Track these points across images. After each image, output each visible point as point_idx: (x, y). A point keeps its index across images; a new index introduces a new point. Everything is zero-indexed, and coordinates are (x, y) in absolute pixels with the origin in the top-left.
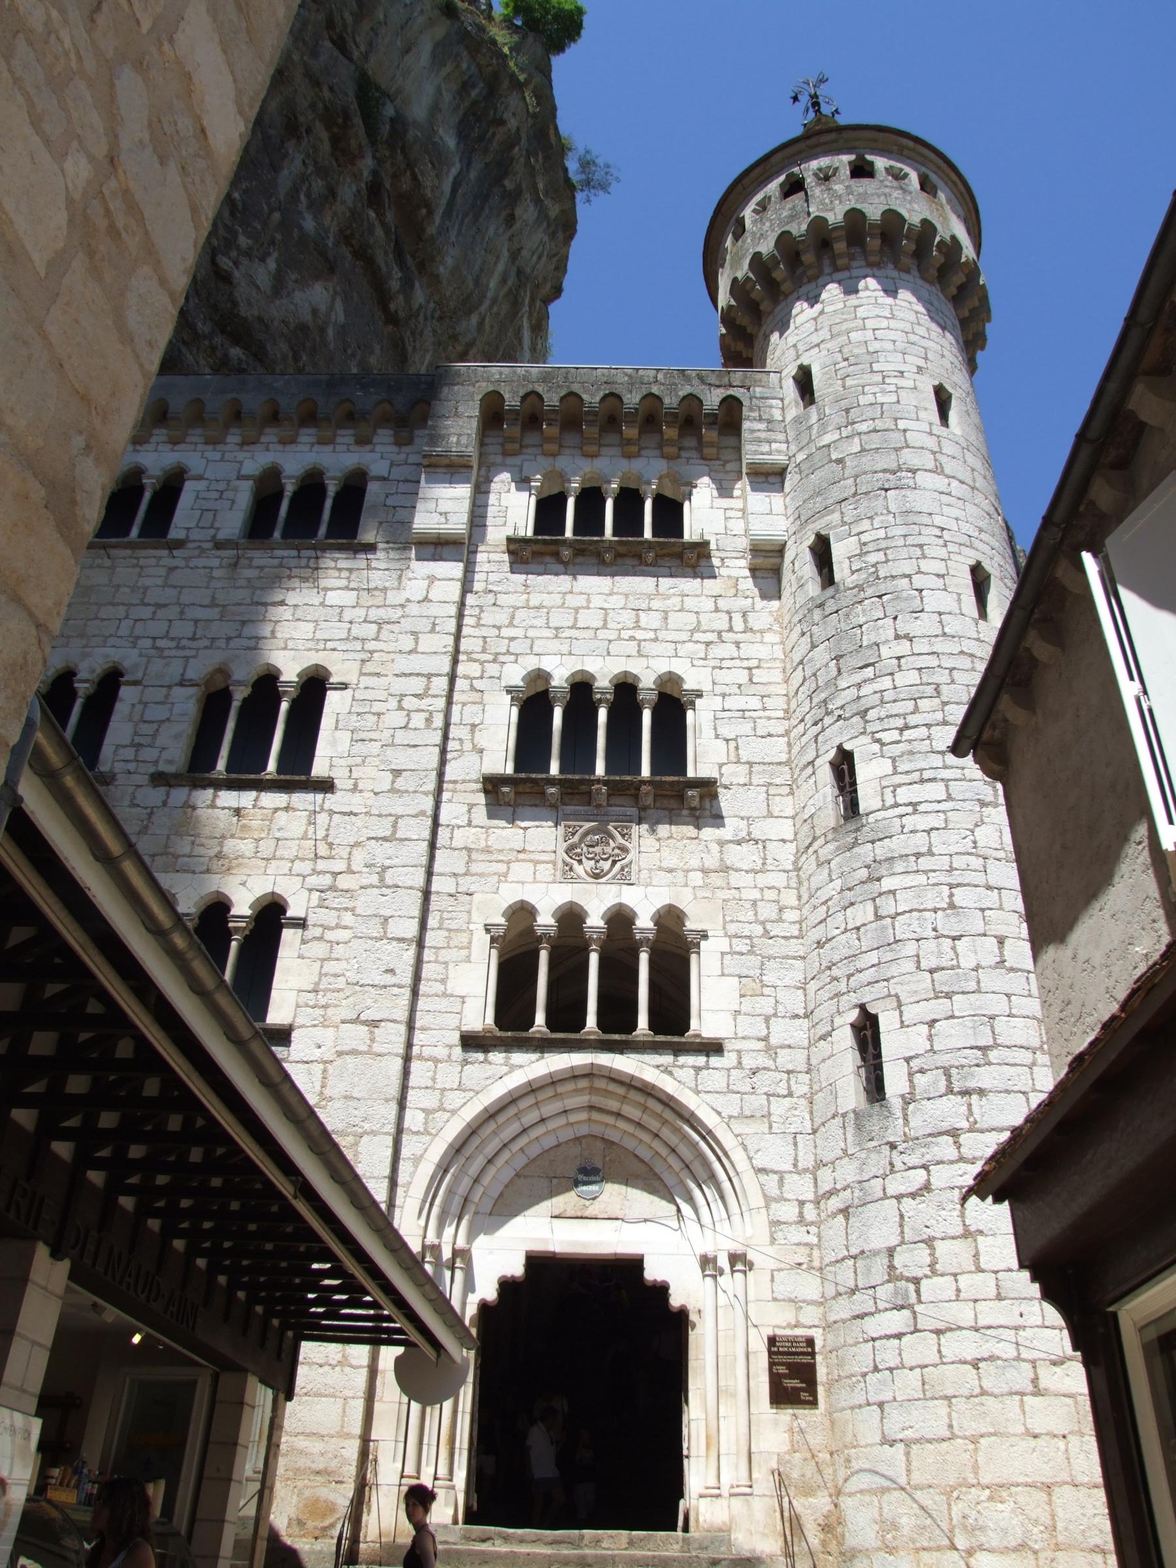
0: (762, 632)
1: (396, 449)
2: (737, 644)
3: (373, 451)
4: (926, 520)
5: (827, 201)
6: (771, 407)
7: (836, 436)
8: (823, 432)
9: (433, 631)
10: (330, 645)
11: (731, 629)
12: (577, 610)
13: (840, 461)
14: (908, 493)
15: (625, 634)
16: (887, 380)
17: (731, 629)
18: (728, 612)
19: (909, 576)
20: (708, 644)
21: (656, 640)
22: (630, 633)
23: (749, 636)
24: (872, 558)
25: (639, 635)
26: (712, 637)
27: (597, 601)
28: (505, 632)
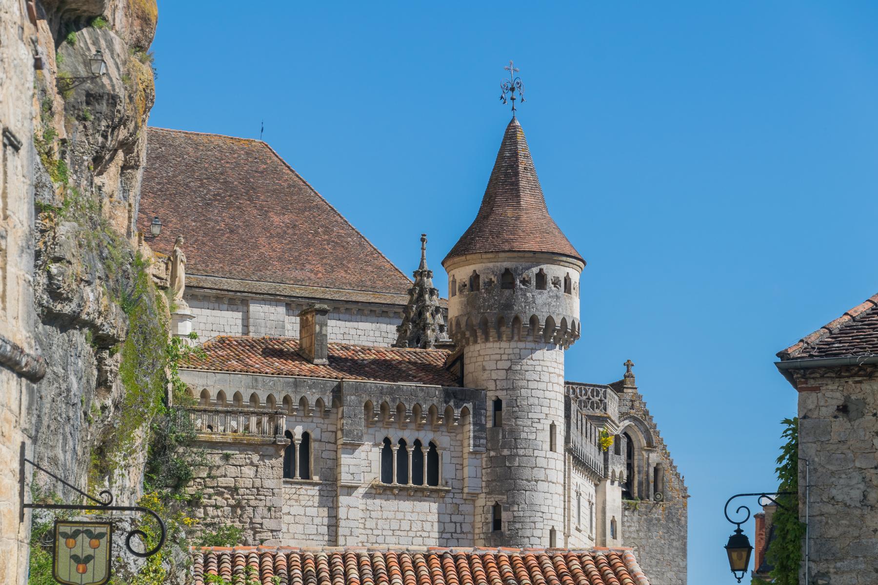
0: (467, 533)
1: (322, 421)
2: (458, 539)
3: (312, 422)
4: (536, 508)
5: (523, 305)
6: (481, 415)
7: (509, 453)
8: (503, 447)
9: (351, 535)
10: (311, 537)
11: (455, 532)
12: (400, 520)
13: (509, 468)
14: (533, 493)
15: (418, 534)
16: (535, 425)
17: (455, 532)
18: (455, 523)
19: (528, 537)
20: (448, 539)
21: (429, 537)
22: (420, 533)
23: (462, 536)
24: (518, 526)
25: (425, 534)
26: (449, 536)
27: (408, 517)
28: (376, 532)
